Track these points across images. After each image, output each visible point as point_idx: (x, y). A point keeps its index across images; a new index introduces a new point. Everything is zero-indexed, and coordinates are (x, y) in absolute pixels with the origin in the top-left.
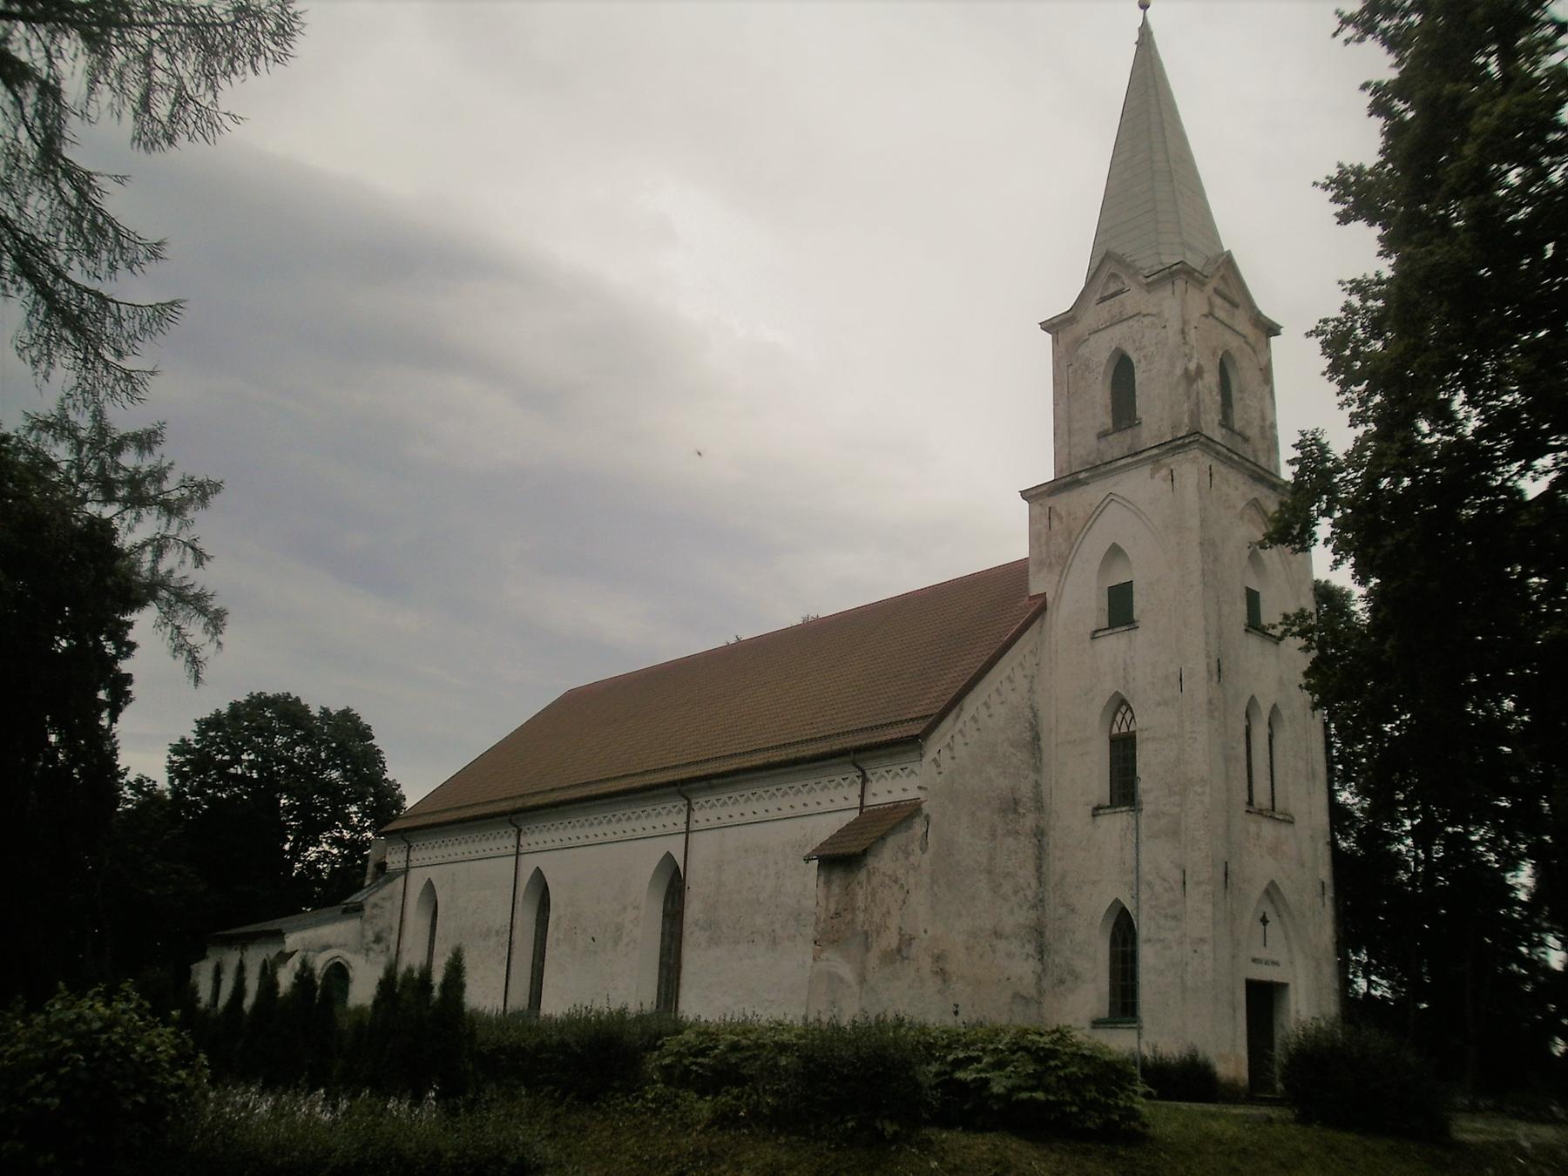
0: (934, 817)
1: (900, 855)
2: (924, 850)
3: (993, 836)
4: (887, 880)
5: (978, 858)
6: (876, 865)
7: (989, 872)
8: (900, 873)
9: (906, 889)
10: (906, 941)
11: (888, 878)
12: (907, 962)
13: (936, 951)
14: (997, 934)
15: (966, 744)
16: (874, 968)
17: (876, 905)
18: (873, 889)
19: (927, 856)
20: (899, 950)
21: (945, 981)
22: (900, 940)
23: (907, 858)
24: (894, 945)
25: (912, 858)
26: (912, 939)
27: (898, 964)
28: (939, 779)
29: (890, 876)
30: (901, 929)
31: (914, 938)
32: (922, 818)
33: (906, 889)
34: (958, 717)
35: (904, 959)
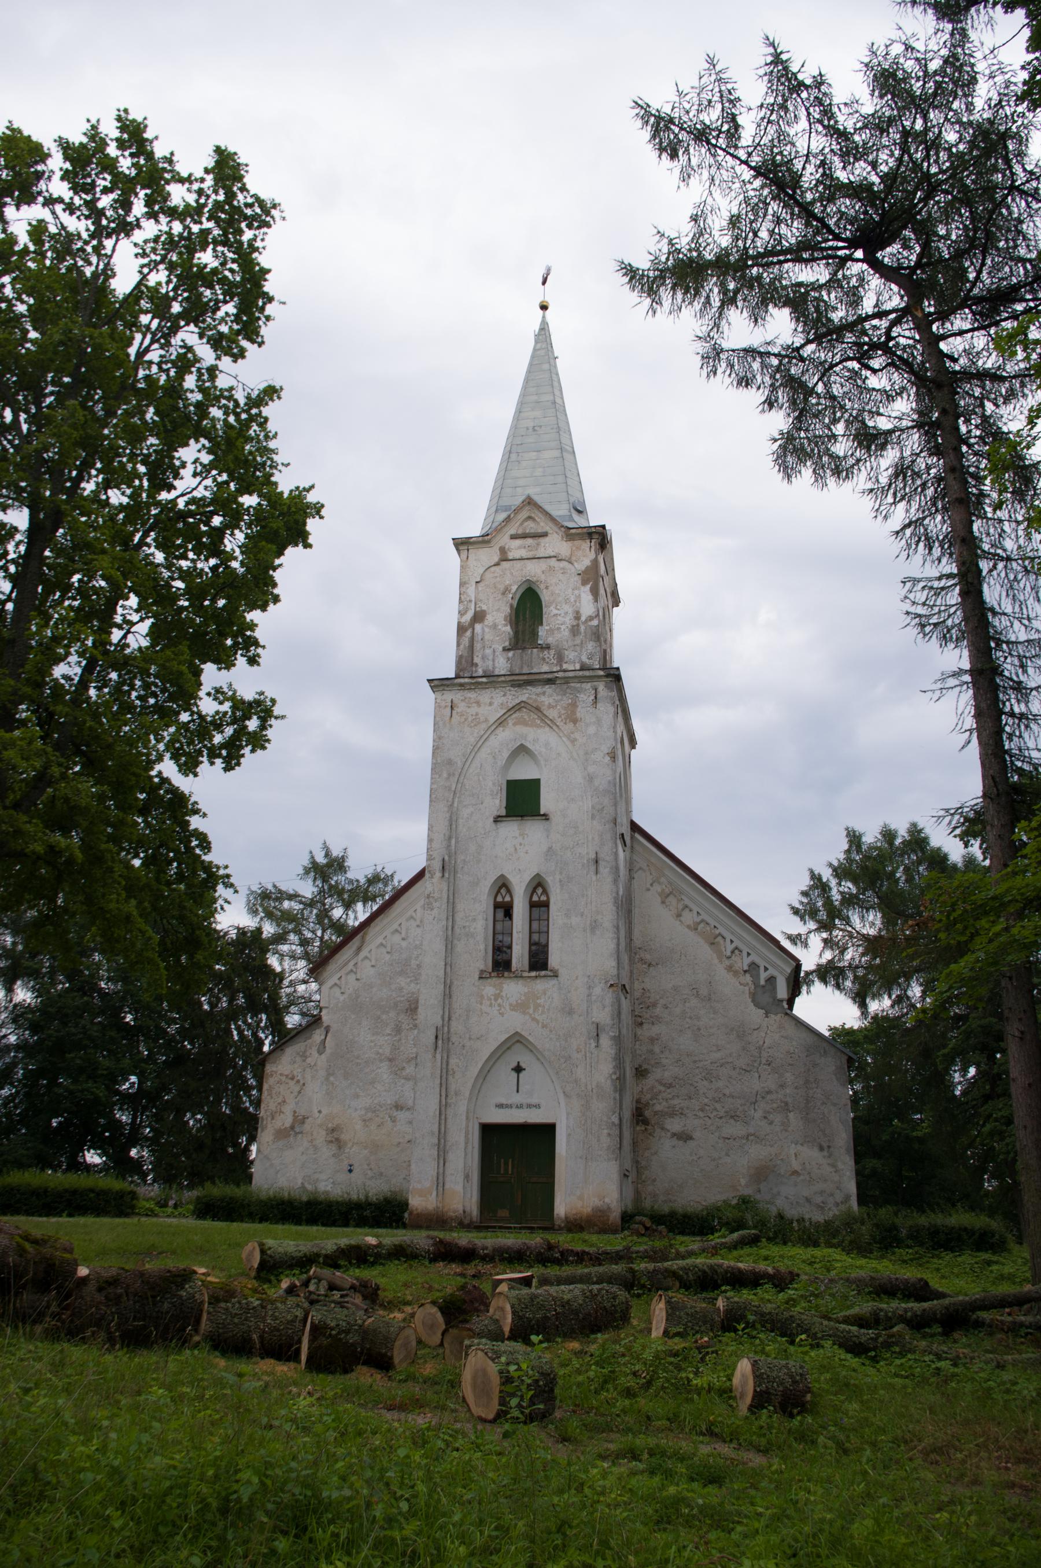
0: (334, 1027)
1: (298, 1059)
2: (320, 1053)
3: (398, 1030)
4: (283, 1078)
7: (390, 1060)
8: (297, 1072)
10: (300, 1120)
14: (398, 1107)
20: (292, 1128)
21: (340, 1148)
24: (288, 1124)
25: (309, 1060)
26: (305, 1118)
27: (292, 1139)
28: (342, 998)
34: (359, 949)
35: (297, 1133)
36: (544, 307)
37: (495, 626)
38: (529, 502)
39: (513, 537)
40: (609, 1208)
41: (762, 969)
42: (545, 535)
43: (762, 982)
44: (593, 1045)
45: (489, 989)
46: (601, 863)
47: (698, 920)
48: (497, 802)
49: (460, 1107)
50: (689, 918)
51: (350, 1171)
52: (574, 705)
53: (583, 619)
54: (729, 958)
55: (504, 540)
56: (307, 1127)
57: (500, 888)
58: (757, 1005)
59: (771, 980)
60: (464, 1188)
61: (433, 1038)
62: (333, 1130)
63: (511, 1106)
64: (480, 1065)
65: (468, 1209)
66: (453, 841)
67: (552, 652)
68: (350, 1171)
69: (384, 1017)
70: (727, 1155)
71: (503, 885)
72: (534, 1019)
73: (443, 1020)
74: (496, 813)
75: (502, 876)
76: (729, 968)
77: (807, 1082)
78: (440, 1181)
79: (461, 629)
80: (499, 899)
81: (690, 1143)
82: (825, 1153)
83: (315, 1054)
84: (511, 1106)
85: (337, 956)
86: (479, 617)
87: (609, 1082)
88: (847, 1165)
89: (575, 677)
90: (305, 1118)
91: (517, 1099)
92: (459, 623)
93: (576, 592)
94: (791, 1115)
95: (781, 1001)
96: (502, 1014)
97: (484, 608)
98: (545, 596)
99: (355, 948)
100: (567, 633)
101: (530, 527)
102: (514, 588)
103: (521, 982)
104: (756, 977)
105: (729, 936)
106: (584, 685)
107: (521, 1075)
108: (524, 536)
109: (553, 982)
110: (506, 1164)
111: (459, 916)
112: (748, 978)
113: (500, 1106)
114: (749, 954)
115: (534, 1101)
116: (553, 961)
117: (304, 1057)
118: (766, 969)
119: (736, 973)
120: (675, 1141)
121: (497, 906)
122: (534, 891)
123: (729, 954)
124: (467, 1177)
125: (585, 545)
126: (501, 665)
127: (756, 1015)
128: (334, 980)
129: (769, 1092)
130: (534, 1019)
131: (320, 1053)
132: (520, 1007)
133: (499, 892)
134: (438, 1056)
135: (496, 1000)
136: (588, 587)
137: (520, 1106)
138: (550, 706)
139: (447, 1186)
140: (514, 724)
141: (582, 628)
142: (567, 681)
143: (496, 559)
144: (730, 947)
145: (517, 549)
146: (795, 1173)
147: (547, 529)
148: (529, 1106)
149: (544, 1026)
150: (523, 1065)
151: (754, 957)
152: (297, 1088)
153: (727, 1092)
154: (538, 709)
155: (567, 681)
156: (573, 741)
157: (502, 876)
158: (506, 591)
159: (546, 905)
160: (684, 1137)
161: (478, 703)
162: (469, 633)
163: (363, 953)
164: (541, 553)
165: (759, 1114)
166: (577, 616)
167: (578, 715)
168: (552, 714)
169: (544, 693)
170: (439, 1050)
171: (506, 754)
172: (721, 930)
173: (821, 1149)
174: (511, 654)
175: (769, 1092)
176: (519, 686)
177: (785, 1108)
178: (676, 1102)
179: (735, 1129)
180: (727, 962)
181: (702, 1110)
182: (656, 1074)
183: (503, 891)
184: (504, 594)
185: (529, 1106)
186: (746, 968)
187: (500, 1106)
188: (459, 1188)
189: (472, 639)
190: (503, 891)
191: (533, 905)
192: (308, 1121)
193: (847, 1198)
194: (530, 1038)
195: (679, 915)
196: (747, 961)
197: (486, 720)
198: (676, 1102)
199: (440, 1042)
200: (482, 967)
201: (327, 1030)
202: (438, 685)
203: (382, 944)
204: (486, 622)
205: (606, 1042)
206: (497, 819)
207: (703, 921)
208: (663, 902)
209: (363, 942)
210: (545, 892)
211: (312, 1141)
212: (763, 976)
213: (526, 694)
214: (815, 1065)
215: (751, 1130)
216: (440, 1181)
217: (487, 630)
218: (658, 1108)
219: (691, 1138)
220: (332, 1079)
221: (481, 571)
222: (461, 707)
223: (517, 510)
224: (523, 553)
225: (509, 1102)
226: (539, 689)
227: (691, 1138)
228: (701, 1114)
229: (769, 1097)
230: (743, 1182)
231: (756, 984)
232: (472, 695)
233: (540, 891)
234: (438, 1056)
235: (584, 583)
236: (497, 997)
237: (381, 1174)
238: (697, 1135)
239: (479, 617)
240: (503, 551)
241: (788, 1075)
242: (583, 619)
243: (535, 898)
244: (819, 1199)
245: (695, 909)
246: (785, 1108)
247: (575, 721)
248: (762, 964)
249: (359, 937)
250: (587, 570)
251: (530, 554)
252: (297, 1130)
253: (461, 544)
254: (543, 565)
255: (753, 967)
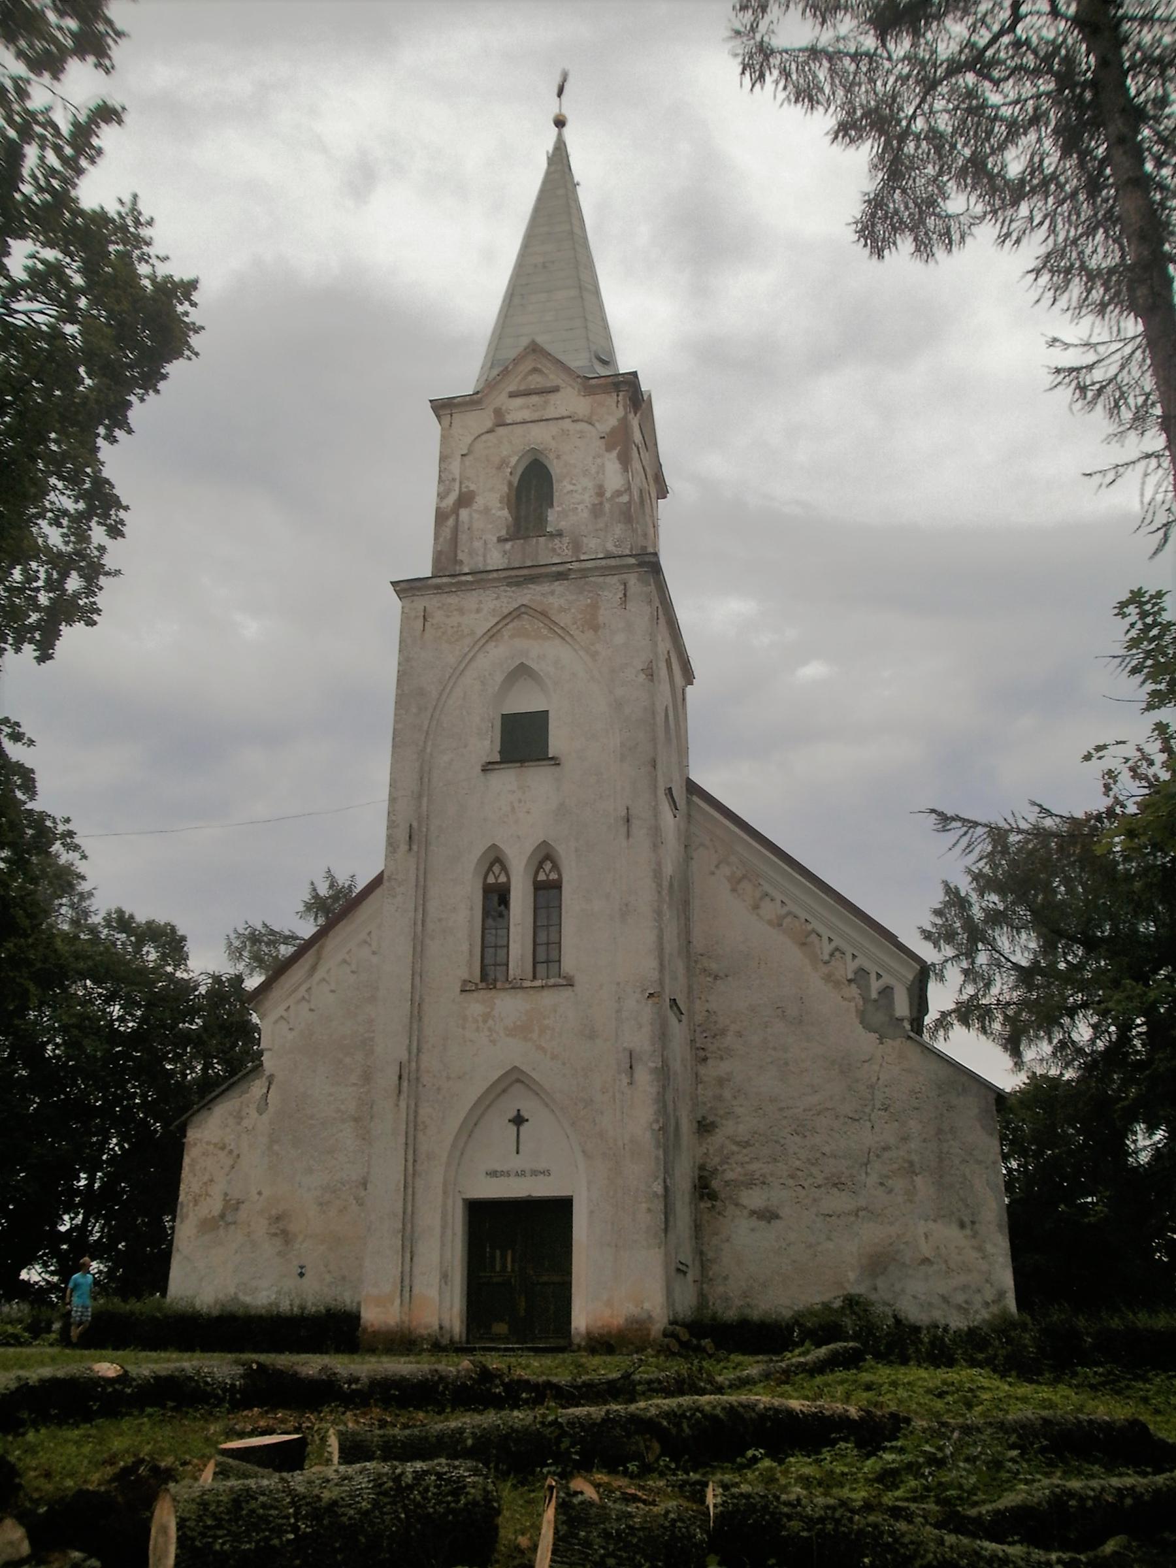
2: (260, 1112)
4: (211, 1148)
5: (342, 1107)
6: (199, 1136)
9: (235, 1153)
11: (212, 1146)
12: (233, 1227)
13: (274, 1212)
15: (333, 991)
16: (189, 1237)
17: (195, 1175)
18: (193, 1160)
19: (265, 1117)
20: (222, 1216)
22: (224, 1206)
23: (239, 1124)
24: (216, 1213)
25: (245, 1123)
26: (239, 1202)
27: (221, 1232)
29: (215, 1145)
30: (226, 1194)
31: (243, 1202)
32: (264, 1079)
33: (235, 1153)
34: (314, 968)
35: (228, 1224)
36: (560, 123)
37: (486, 511)
38: (534, 349)
39: (512, 395)
40: (650, 1317)
41: (873, 976)
42: (555, 390)
43: (874, 995)
44: (625, 1080)
45: (475, 1006)
46: (635, 823)
47: (784, 911)
48: (487, 743)
49: (434, 1177)
50: (769, 910)
51: (301, 1275)
52: (594, 607)
53: (608, 495)
54: (826, 963)
55: (500, 399)
56: (242, 1215)
57: (492, 865)
58: (868, 1027)
59: (887, 991)
60: (440, 1293)
61: (396, 1078)
62: (278, 1218)
63: (507, 1174)
64: (462, 1115)
65: (446, 1324)
66: (425, 800)
67: (566, 540)
68: (301, 1275)
69: (348, 1060)
70: (829, 1239)
71: (496, 860)
72: (540, 1048)
73: (410, 1053)
74: (486, 759)
75: (494, 846)
76: (828, 978)
77: (940, 1131)
78: (406, 1284)
79: (441, 517)
80: (491, 880)
81: (777, 1224)
82: (968, 1232)
83: (254, 1114)
84: (508, 1174)
85: (283, 978)
86: (465, 500)
87: (648, 1135)
88: (999, 1246)
89: (596, 568)
90: (239, 1202)
91: (516, 1163)
92: (438, 510)
93: (599, 461)
94: (918, 1180)
95: (902, 1020)
96: (493, 1042)
97: (473, 487)
98: (556, 469)
99: (307, 967)
100: (585, 514)
101: (536, 381)
102: (514, 460)
103: (520, 994)
104: (865, 989)
105: (825, 933)
106: (608, 579)
107: (523, 1128)
108: (527, 393)
109: (567, 993)
110: (504, 1257)
111: (432, 906)
112: (854, 990)
113: (493, 1174)
114: (854, 956)
115: (542, 1166)
116: (569, 962)
117: (239, 1118)
118: (879, 976)
119: (837, 984)
120: (754, 1222)
121: (488, 890)
122: (540, 866)
123: (826, 957)
124: (445, 1277)
125: (611, 400)
126: (496, 559)
127: (867, 1041)
128: (280, 1011)
129: (886, 1148)
130: (540, 1048)
131: (260, 1112)
132: (521, 1030)
133: (490, 869)
134: (403, 1104)
135: (485, 1022)
136: (614, 454)
137: (521, 1174)
138: (561, 610)
139: (416, 1290)
140: (512, 637)
141: (607, 506)
142: (584, 574)
143: (489, 424)
144: (828, 948)
145: (517, 409)
146: (926, 1261)
147: (559, 382)
148: (535, 1173)
149: (554, 1057)
150: (525, 1114)
151: (861, 961)
152: (230, 1162)
153: (826, 1149)
154: (544, 614)
155: (584, 574)
156: (594, 655)
157: (494, 846)
158: (503, 463)
159: (557, 886)
160: (768, 1215)
161: (461, 611)
162: (451, 522)
163: (320, 973)
164: (551, 413)
165: (873, 1179)
166: (600, 491)
167: (601, 619)
168: (564, 619)
169: (552, 593)
170: (404, 1096)
171: (499, 678)
172: (816, 925)
173: (962, 1226)
174: (508, 546)
175: (886, 1148)
176: (518, 584)
177: (910, 1170)
178: (754, 1166)
179: (839, 1201)
180: (825, 970)
181: (792, 1177)
182: (728, 1128)
183: (496, 868)
184: (499, 468)
185: (535, 1173)
186: (850, 976)
187: (493, 1174)
188: (433, 1293)
189: (456, 530)
190: (496, 868)
191: (539, 887)
192: (242, 1207)
193: (1001, 1295)
194: (534, 1075)
195: (756, 907)
196: (852, 966)
197: (472, 633)
198: (754, 1166)
199: (405, 1084)
200: (466, 976)
201: (271, 1080)
202: (406, 588)
203: (344, 961)
204: (475, 506)
205: (643, 1076)
206: (487, 768)
207: (789, 913)
208: (734, 890)
209: (319, 957)
210: (556, 867)
211: (249, 1235)
212: (875, 986)
213: (529, 595)
214: (950, 1108)
215: (862, 1203)
216: (406, 1284)
217: (476, 516)
218: (730, 1176)
219: (777, 1217)
220: (276, 1147)
221: (469, 440)
222: (438, 617)
223: (517, 361)
224: (526, 415)
225: (505, 1168)
226: (545, 588)
227: (777, 1217)
228: (791, 1182)
229: (887, 1155)
230: (852, 1276)
231: (866, 999)
232: (452, 600)
233: (548, 866)
234: (403, 1104)
235: (609, 449)
236: (486, 1017)
237: (344, 1278)
238: (785, 1212)
239: (465, 500)
240: (498, 412)
241: (912, 1123)
242: (608, 495)
243: (542, 877)
244: (960, 1298)
245: (779, 897)
246: (910, 1170)
247: (596, 628)
248: (872, 969)
249: (312, 952)
250: (613, 431)
251: (536, 416)
252: (229, 1219)
253: (443, 408)
254: (554, 428)
255: (862, 972)
